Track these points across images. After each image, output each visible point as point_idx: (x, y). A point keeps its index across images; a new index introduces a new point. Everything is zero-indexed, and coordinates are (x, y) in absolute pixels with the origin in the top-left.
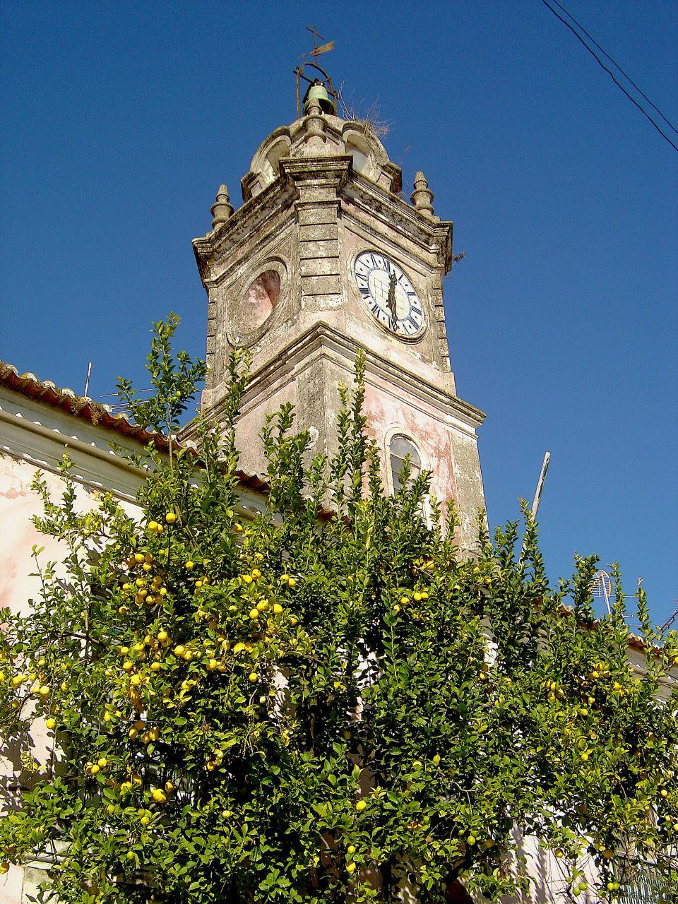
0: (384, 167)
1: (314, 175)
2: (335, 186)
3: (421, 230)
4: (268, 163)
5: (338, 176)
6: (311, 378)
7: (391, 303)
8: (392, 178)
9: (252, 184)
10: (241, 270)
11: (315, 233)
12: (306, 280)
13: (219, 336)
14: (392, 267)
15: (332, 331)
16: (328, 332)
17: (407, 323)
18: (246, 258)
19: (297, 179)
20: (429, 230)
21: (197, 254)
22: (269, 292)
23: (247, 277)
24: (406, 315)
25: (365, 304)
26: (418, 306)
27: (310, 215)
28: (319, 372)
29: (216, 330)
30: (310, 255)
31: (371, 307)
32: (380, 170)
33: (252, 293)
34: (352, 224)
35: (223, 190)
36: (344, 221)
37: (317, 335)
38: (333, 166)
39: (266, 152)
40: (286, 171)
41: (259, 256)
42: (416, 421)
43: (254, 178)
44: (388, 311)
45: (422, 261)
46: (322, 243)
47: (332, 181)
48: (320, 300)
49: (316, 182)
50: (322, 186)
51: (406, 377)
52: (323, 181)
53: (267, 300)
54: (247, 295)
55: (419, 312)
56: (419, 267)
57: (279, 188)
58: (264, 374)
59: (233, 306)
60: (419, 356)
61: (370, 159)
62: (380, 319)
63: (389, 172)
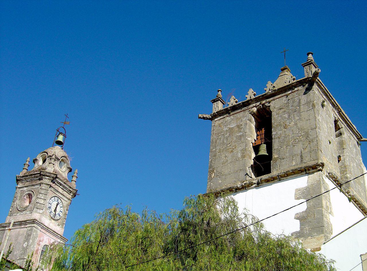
0: (68, 168)
1: (47, 176)
2: (51, 180)
3: (70, 190)
4: (41, 157)
5: (53, 178)
6: (29, 230)
7: (55, 210)
8: (69, 170)
9: (36, 161)
10: (25, 189)
11: (43, 192)
12: (36, 204)
13: (15, 203)
14: (59, 200)
15: (38, 221)
16: (36, 221)
17: (58, 215)
18: (27, 187)
19: (44, 176)
20: (72, 190)
21: (17, 179)
22: (29, 197)
23: (26, 192)
24: (58, 213)
25: (48, 211)
26: (62, 211)
27: (44, 186)
28: (31, 230)
29: (15, 201)
30: (40, 198)
31: (50, 212)
32: (67, 168)
33: (26, 196)
34: (53, 189)
35: (28, 160)
36: (51, 189)
37: (34, 221)
38: (52, 175)
39: (41, 155)
40: (42, 173)
41: (30, 188)
42: (51, 241)
43: (37, 160)
44: (54, 213)
45: (67, 198)
46: (43, 195)
47: (51, 179)
48: (38, 210)
49: (47, 178)
50: (48, 179)
51: (52, 231)
52: (49, 178)
53: (29, 199)
54: (24, 196)
55: (61, 212)
56: (66, 199)
57: (39, 175)
58: (21, 223)
59: (21, 197)
60: (57, 224)
61: (66, 164)
62: (51, 215)
63: (69, 169)
